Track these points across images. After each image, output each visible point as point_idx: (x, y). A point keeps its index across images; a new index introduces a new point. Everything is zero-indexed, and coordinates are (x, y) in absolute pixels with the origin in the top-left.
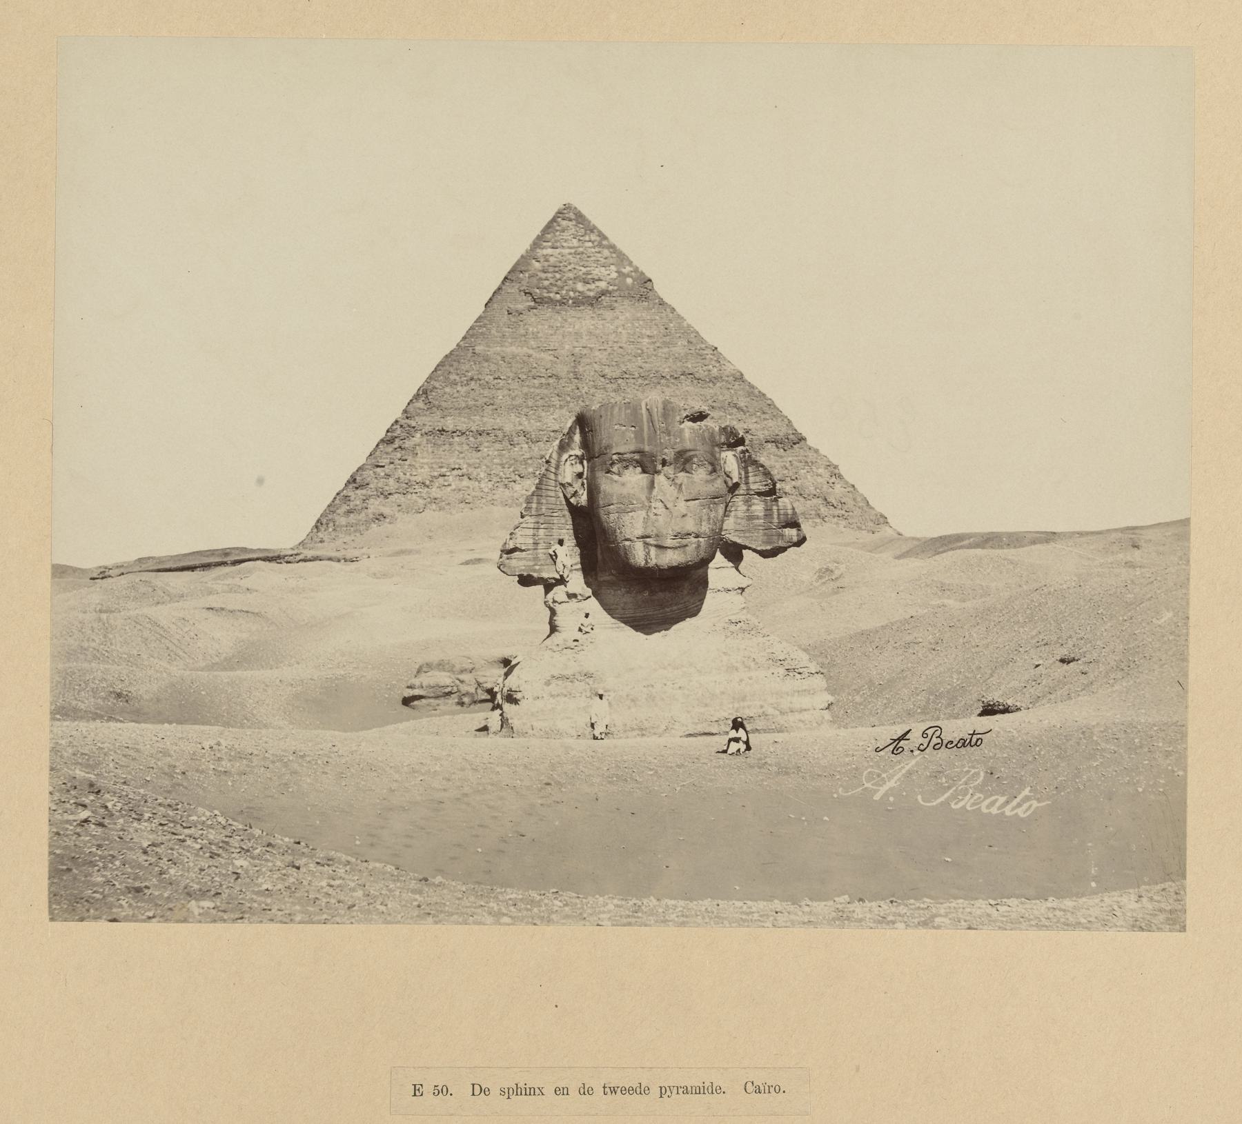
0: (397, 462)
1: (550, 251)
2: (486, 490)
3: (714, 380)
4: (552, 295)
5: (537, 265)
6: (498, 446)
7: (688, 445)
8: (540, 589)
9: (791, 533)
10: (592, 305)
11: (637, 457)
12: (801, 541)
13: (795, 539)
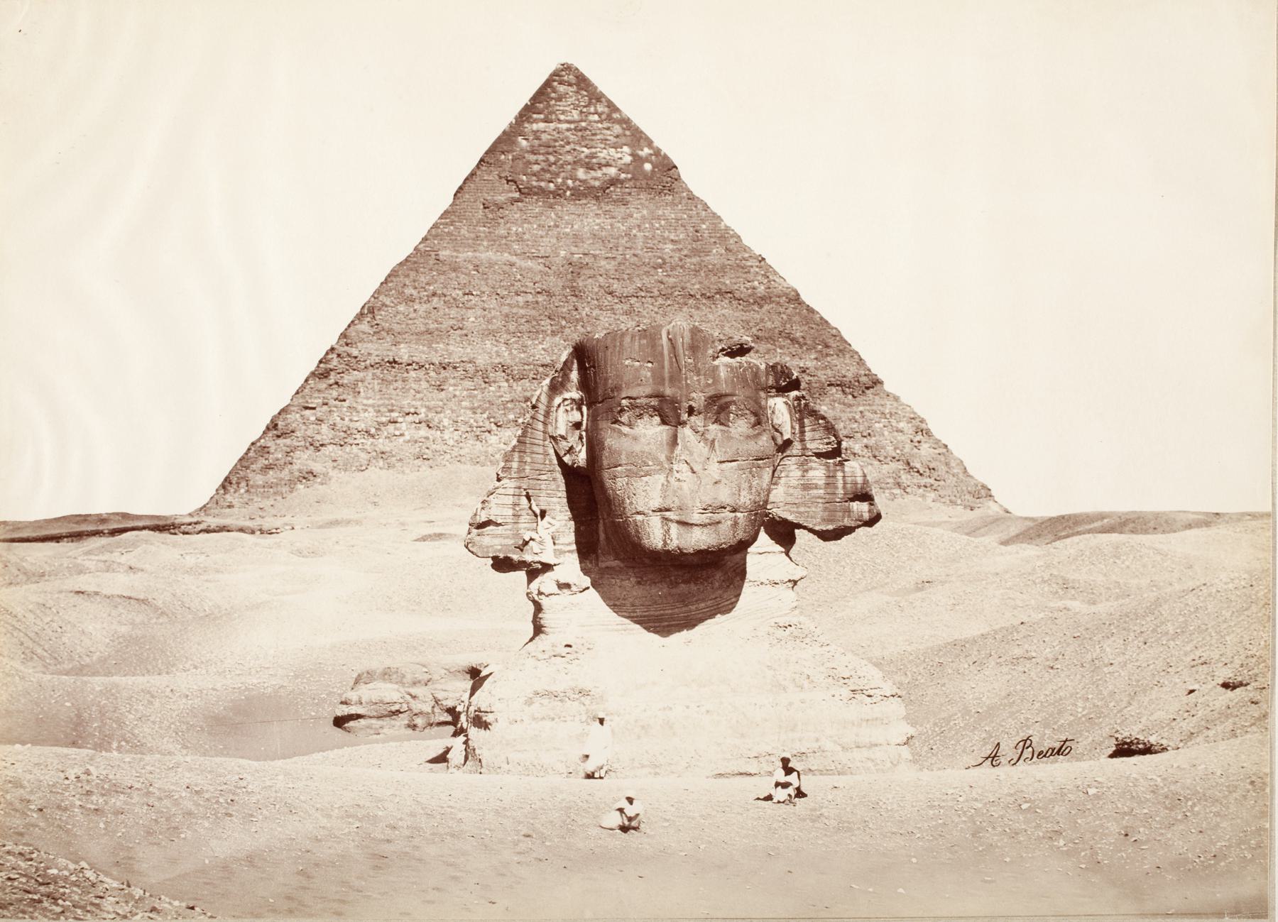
0: (332, 402)
1: (542, 125)
2: (451, 442)
3: (761, 301)
4: (543, 184)
5: (524, 143)
6: (468, 384)
7: (724, 388)
8: (521, 575)
9: (861, 508)
10: (597, 198)
11: (654, 402)
12: (874, 520)
13: (866, 516)
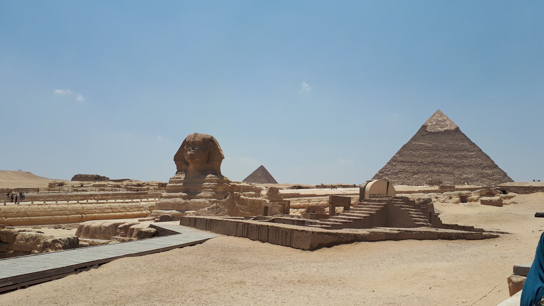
3: (473, 151)
